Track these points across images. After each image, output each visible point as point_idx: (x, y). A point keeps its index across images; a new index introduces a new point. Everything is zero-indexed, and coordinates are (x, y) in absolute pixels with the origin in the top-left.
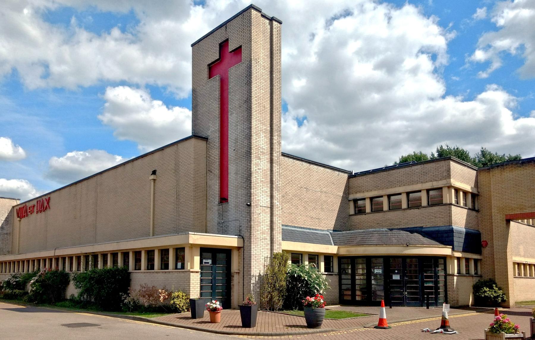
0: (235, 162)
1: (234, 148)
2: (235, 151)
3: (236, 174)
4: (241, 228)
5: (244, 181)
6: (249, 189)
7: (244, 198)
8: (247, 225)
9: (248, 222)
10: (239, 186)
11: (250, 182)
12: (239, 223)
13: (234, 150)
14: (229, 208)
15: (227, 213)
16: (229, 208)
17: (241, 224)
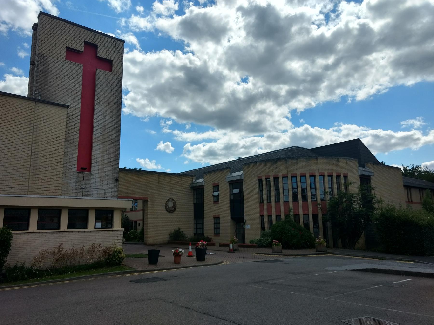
0: (101, 143)
1: (101, 132)
2: (102, 135)
3: (103, 152)
4: (106, 196)
5: (112, 161)
6: (117, 168)
7: (111, 174)
8: (113, 195)
9: (115, 192)
10: (106, 163)
11: (118, 163)
12: (104, 192)
13: (101, 133)
14: (92, 178)
15: (89, 181)
16: (92, 178)
17: (106, 193)
